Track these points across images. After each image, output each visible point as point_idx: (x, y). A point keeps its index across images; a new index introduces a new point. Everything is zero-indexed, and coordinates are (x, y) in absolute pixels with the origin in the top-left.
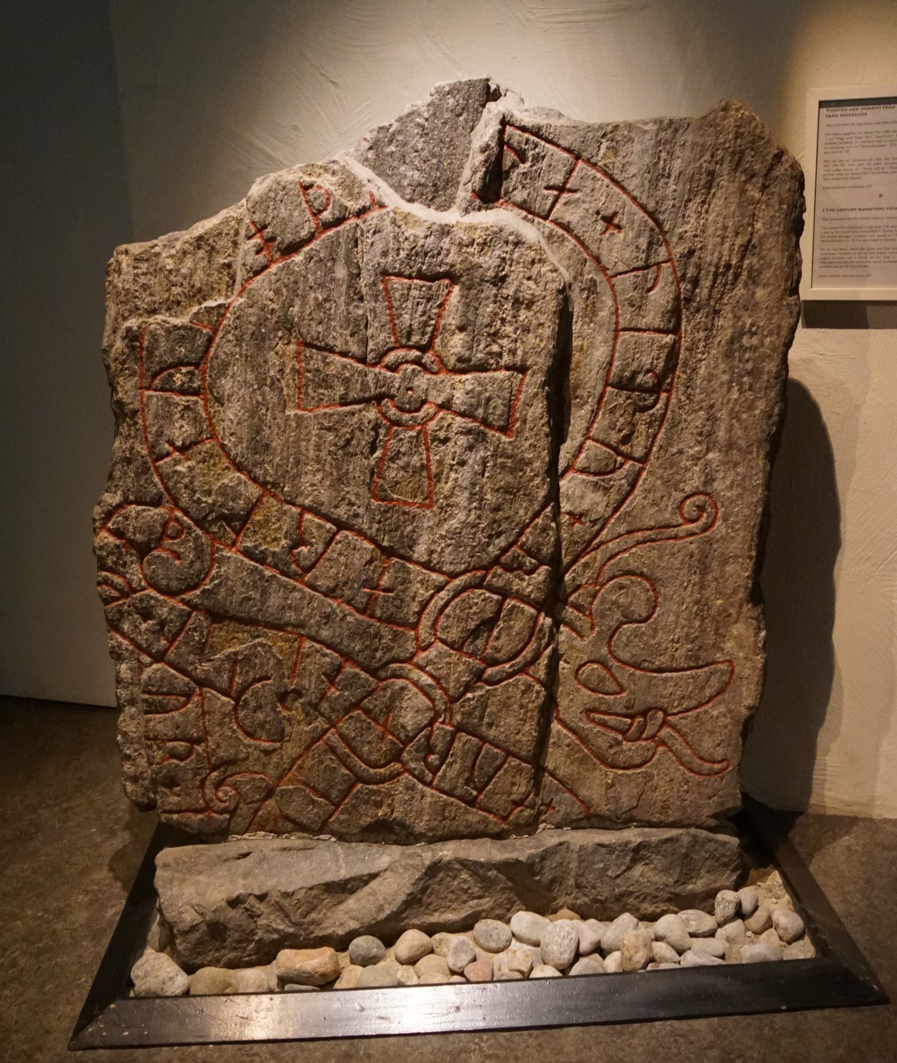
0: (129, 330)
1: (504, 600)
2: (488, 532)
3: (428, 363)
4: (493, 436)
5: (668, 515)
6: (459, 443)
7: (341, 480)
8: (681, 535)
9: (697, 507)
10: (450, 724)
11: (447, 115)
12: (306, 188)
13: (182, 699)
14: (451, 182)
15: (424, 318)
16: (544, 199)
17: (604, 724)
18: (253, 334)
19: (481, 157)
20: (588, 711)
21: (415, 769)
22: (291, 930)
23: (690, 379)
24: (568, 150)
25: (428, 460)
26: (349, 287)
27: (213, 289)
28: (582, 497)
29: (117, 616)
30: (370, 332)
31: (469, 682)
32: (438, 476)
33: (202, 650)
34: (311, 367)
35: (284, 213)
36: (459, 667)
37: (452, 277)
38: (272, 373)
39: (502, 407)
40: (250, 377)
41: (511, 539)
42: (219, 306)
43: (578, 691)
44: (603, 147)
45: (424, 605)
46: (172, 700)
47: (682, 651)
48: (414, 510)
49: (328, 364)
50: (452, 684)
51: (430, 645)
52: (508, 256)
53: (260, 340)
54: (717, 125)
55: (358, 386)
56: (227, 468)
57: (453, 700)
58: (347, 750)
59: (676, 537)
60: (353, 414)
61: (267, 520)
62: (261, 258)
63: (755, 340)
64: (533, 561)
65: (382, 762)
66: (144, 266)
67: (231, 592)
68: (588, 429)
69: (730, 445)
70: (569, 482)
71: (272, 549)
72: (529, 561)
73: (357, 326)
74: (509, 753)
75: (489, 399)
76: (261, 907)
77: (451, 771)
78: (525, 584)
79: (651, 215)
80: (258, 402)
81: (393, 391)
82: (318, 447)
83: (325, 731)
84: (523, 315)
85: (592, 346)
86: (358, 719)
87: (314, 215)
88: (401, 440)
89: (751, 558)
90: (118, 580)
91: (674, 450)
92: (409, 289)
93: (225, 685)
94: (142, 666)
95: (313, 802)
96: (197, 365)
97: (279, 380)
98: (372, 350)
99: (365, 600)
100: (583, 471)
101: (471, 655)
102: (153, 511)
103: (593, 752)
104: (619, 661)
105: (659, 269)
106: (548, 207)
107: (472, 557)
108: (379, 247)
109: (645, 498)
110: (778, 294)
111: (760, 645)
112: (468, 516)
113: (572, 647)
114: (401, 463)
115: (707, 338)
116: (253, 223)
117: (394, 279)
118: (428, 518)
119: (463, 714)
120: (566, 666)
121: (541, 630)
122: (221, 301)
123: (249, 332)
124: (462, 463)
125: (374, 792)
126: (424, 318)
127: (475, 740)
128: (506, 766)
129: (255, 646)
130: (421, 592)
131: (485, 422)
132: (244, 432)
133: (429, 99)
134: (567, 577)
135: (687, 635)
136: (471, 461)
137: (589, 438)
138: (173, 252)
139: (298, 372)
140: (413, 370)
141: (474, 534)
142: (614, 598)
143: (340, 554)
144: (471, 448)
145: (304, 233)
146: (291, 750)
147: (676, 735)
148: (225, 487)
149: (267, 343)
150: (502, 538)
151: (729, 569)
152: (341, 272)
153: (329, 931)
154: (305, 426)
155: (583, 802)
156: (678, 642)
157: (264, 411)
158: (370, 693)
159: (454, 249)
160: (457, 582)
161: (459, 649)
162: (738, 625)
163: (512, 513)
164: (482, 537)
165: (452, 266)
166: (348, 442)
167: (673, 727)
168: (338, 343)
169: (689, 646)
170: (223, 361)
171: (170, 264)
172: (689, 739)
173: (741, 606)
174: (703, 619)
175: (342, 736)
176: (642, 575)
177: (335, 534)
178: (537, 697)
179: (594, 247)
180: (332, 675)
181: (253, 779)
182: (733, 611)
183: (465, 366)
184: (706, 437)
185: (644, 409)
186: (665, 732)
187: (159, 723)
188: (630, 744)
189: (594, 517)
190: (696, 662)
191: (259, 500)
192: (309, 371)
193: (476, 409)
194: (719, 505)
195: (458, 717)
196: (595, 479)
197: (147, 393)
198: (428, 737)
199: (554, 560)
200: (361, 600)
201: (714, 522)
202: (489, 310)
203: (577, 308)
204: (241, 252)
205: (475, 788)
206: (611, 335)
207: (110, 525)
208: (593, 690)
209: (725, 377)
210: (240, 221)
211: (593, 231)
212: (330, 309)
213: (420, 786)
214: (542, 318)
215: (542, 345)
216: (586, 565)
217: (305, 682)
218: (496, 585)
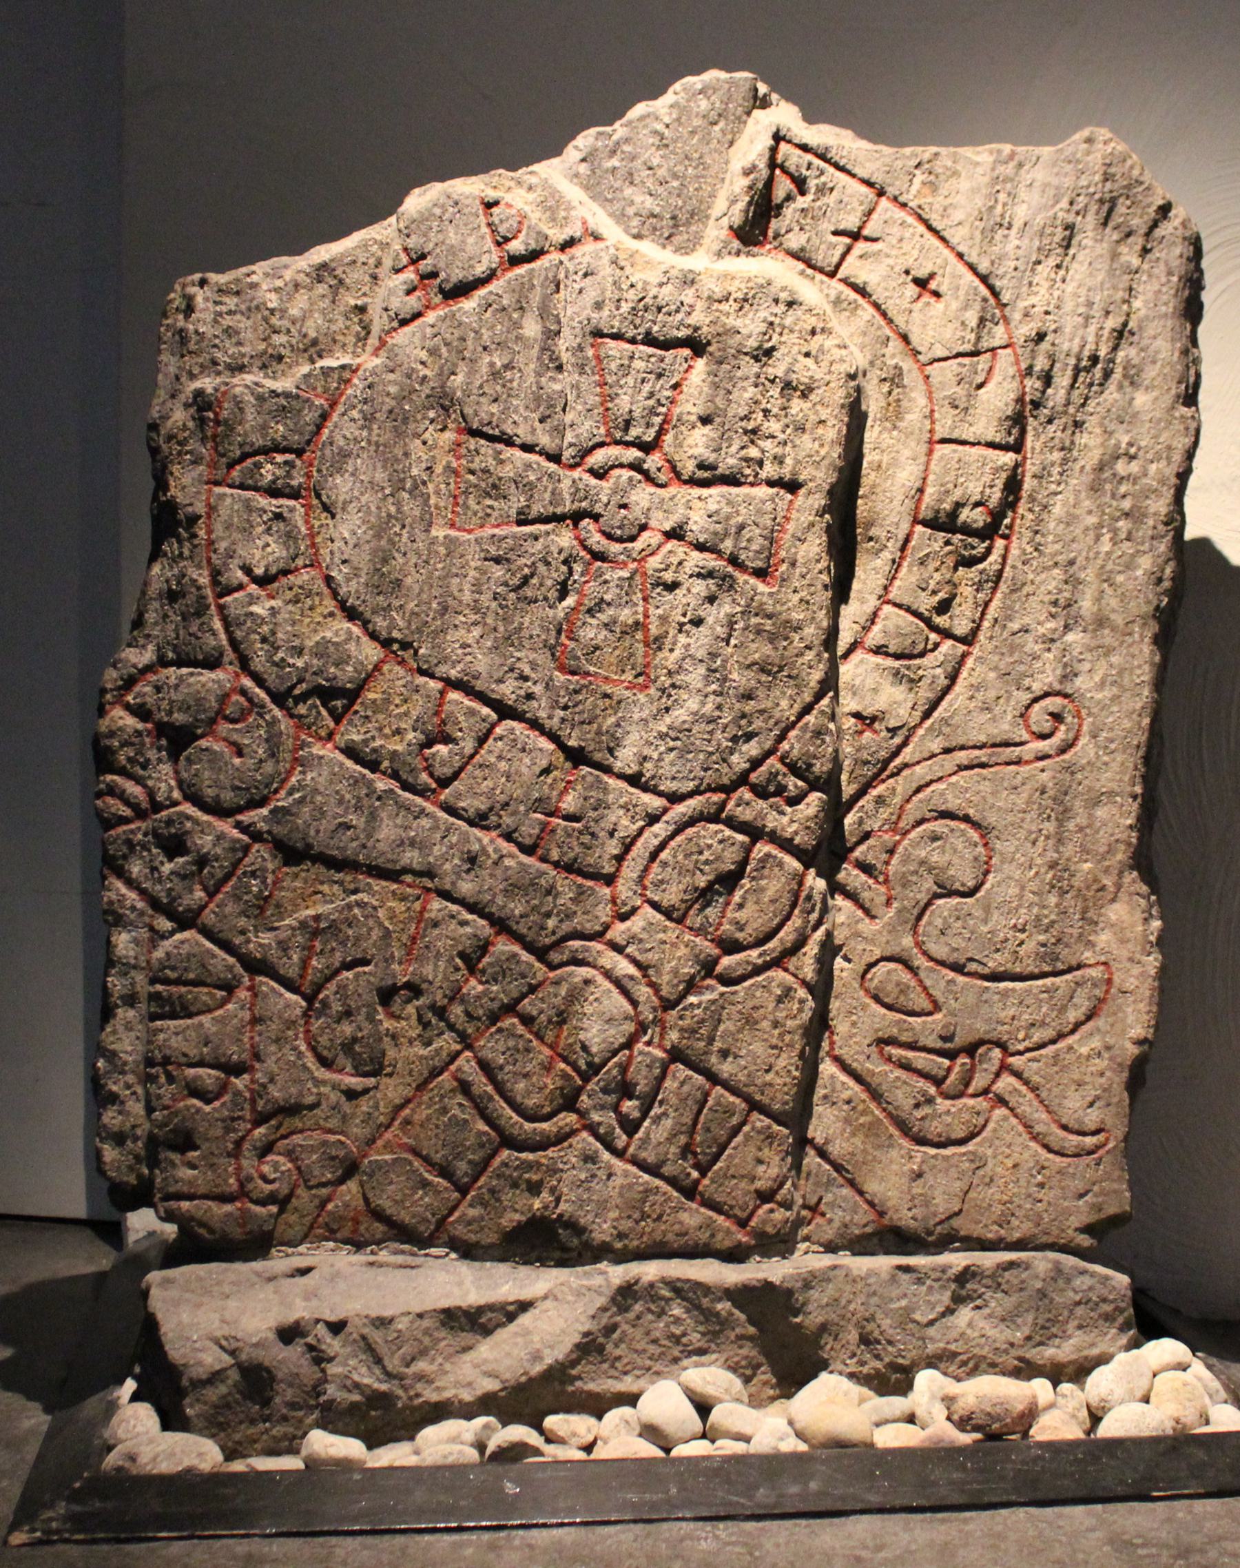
0: (199, 393)
1: (754, 843)
2: (732, 730)
3: (653, 470)
4: (746, 582)
5: (1006, 727)
6: (694, 591)
7: (511, 639)
8: (1026, 758)
9: (1051, 714)
10: (660, 1046)
11: (697, 122)
12: (489, 205)
13: (220, 994)
14: (697, 215)
15: (651, 402)
16: (829, 250)
17: (906, 1066)
18: (391, 412)
19: (746, 182)
20: (882, 1042)
21: (599, 1124)
22: (384, 1387)
23: (1039, 521)
25: (646, 616)
26: (544, 349)
27: (335, 341)
28: (876, 690)
29: (125, 849)
30: (569, 417)
31: (693, 977)
33: (262, 909)
34: (475, 466)
35: (452, 237)
36: (677, 952)
37: (697, 346)
38: (415, 472)
39: (761, 540)
40: (380, 476)
41: (768, 745)
42: (343, 367)
43: (864, 1007)
44: (917, 181)
45: (627, 847)
47: (1030, 946)
48: (619, 692)
49: (502, 462)
50: (666, 978)
51: (634, 910)
52: (777, 321)
53: (400, 420)
54: (1078, 162)
55: (547, 496)
56: (331, 614)
58: (489, 1089)
59: (1018, 762)
60: (536, 539)
61: (387, 701)
62: (413, 302)
63: (1134, 467)
64: (800, 783)
65: (547, 1110)
66: (231, 302)
67: (320, 812)
68: (886, 588)
69: (1101, 622)
70: (857, 666)
71: (391, 747)
72: (794, 784)
73: (549, 409)
74: (754, 1106)
75: (741, 527)
76: (333, 1345)
77: (658, 1133)
78: (785, 820)
79: (984, 279)
80: (389, 516)
81: (598, 508)
82: (477, 588)
83: (454, 1057)
84: (797, 405)
85: (894, 463)
86: (511, 1033)
87: (499, 244)
88: (606, 582)
89: (1135, 797)
91: (1015, 626)
92: (632, 358)
93: (292, 972)
94: (158, 936)
95: (425, 1184)
96: (299, 453)
97: (424, 483)
98: (571, 445)
99: (536, 831)
100: (878, 650)
101: (698, 931)
102: (207, 676)
103: (890, 1115)
104: (931, 959)
105: (994, 357)
106: (835, 260)
107: (706, 770)
108: (591, 295)
109: (972, 697)
110: (1168, 399)
111: (1152, 938)
112: (703, 704)
113: (857, 934)
114: (603, 617)
115: (1065, 461)
116: (406, 249)
117: (611, 343)
119: (682, 1030)
120: (846, 965)
121: (809, 898)
122: (346, 360)
123: (385, 408)
124: (698, 622)
125: (529, 1166)
126: (651, 402)
127: (699, 1079)
128: (746, 1128)
129: (349, 907)
130: (625, 822)
131: (734, 561)
132: (363, 559)
134: (849, 820)
135: (1038, 918)
136: (710, 620)
137: (888, 602)
138: (279, 283)
139: (456, 473)
140: (630, 479)
141: (711, 733)
142: (923, 854)
143: (500, 758)
144: (711, 599)
145: (480, 270)
146: (392, 1090)
147: (1023, 1089)
148: (326, 642)
149: (412, 426)
150: (753, 742)
151: (1100, 813)
152: (532, 328)
153: (447, 1394)
154: (458, 552)
155: (871, 1204)
156: (1023, 931)
157: (397, 529)
158: (533, 989)
159: (700, 305)
160: (681, 809)
161: (680, 921)
162: (1116, 906)
163: (770, 704)
165: (696, 329)
166: (525, 581)
167: (1018, 1075)
168: (520, 432)
169: (1042, 938)
170: (341, 449)
171: (273, 301)
172: (1044, 1095)
173: (1120, 874)
174: (1063, 893)
176: (966, 819)
177: (493, 726)
178: (800, 1010)
179: (900, 320)
180: (471, 959)
181: (325, 1143)
182: (1108, 881)
183: (709, 476)
184: (1064, 608)
185: (970, 562)
186: (1006, 1083)
187: (176, 1035)
188: (948, 1102)
189: (893, 723)
190: (1054, 965)
191: (377, 668)
192: (472, 472)
193: (722, 541)
194: (1084, 712)
195: (674, 1036)
196: (897, 664)
197: (218, 490)
198: (624, 1068)
199: (829, 784)
200: (528, 832)
201: (1076, 738)
202: (747, 395)
203: (873, 405)
204: (381, 292)
205: (696, 1166)
206: (924, 448)
207: (130, 698)
208: (889, 1007)
209: (1092, 520)
210: (384, 246)
211: (899, 297)
212: (511, 381)
213: (606, 1155)
214: (824, 413)
215: (823, 452)
216: (880, 801)
217: (428, 971)
218: (743, 818)
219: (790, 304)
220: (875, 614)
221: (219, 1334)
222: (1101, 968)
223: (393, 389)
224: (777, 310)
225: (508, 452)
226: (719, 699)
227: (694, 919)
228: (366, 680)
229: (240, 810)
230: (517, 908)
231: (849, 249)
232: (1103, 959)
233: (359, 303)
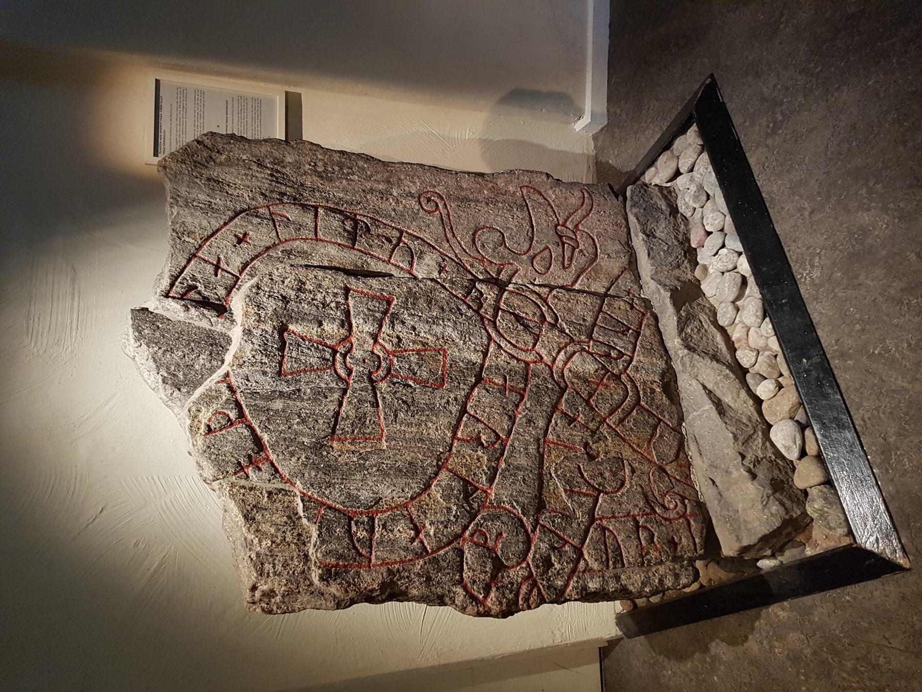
0: (321, 578)
10: (589, 342)
11: (157, 334)
12: (209, 430)
13: (607, 533)
16: (224, 278)
17: (571, 259)
19: (193, 310)
20: (564, 267)
22: (760, 433)
23: (347, 202)
24: (189, 261)
25: (413, 350)
26: (290, 398)
27: (288, 507)
29: (552, 590)
30: (323, 385)
32: (424, 344)
33: (567, 516)
35: (228, 448)
36: (550, 337)
37: (282, 329)
38: (355, 459)
39: (374, 302)
42: (302, 501)
43: (552, 273)
44: (187, 239)
45: (513, 357)
46: (609, 541)
48: (448, 361)
49: (347, 416)
53: (329, 469)
54: (176, 173)
55: (363, 393)
59: (448, 215)
62: (265, 466)
63: (320, 164)
66: (268, 567)
68: (383, 261)
71: (486, 461)
72: (474, 293)
73: (319, 394)
74: (600, 310)
75: (369, 309)
77: (620, 344)
79: (237, 214)
81: (366, 372)
82: (410, 425)
83: (610, 427)
84: (309, 286)
85: (327, 255)
87: (232, 424)
90: (524, 589)
93: (591, 500)
94: (588, 569)
95: (661, 436)
96: (350, 519)
100: (411, 264)
101: (541, 331)
102: (467, 554)
103: (590, 265)
104: (529, 249)
106: (230, 276)
108: (259, 377)
114: (416, 369)
116: (235, 473)
117: (285, 366)
118: (453, 352)
122: (298, 500)
124: (414, 328)
125: (645, 393)
129: (558, 476)
131: (385, 313)
132: (401, 481)
133: (144, 347)
136: (412, 323)
138: (256, 541)
143: (484, 411)
144: (403, 323)
145: (246, 433)
146: (627, 453)
152: (278, 405)
153: (752, 409)
154: (394, 435)
155: (622, 272)
158: (578, 393)
159: (262, 326)
160: (493, 335)
161: (538, 336)
165: (274, 328)
166: (404, 402)
167: (566, 221)
171: (267, 543)
175: (611, 414)
179: (259, 250)
181: (654, 481)
183: (346, 323)
184: (384, 195)
185: (368, 230)
187: (629, 553)
189: (440, 260)
190: (524, 206)
191: (451, 471)
195: (583, 338)
196: (415, 258)
197: (373, 560)
198: (600, 356)
200: (514, 397)
207: (481, 597)
208: (550, 265)
209: (344, 182)
210: (233, 485)
211: (247, 251)
213: (634, 363)
217: (577, 439)
219: (259, 288)
220: (395, 265)
221: (760, 507)
223: (313, 474)
224: (262, 294)
225: (343, 414)
227: (536, 331)
228: (458, 476)
229: (526, 531)
231: (223, 270)
233: (266, 495)
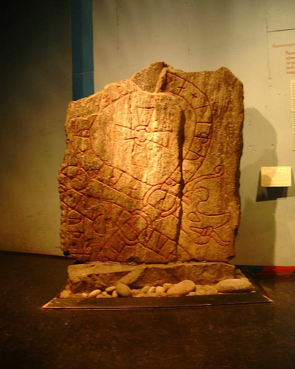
14: (154, 86)
17: (195, 231)
21: (141, 241)
24: (183, 78)
32: (149, 159)
41: (169, 176)
42: (96, 115)
43: (188, 221)
46: (76, 221)
56: (95, 157)
57: (152, 221)
62: (106, 104)
63: (232, 125)
66: (77, 105)
67: (94, 190)
69: (227, 153)
72: (174, 183)
74: (169, 238)
76: (96, 278)
83: (118, 230)
85: (190, 127)
90: (64, 187)
91: (212, 154)
93: (90, 217)
96: (88, 129)
101: (158, 209)
104: (200, 212)
105: (207, 108)
108: (136, 101)
110: (238, 113)
115: (220, 125)
118: (146, 171)
122: (96, 114)
127: (159, 233)
129: (99, 206)
132: (100, 147)
133: (149, 67)
145: (117, 98)
146: (108, 236)
151: (228, 186)
164: (161, 176)
167: (215, 232)
169: (218, 208)
171: (83, 105)
174: (222, 200)
175: (122, 231)
179: (190, 103)
180: (120, 213)
184: (221, 151)
186: (213, 233)
191: (103, 165)
195: (154, 226)
198: (146, 232)
200: (128, 192)
202: (163, 116)
204: (101, 102)
206: (195, 124)
209: (225, 135)
214: (177, 118)
217: (112, 216)
221: (78, 276)
222: (229, 213)
226: (160, 169)
227: (157, 207)
229: (81, 190)
230: (127, 205)
231: (181, 90)
232: (229, 212)
